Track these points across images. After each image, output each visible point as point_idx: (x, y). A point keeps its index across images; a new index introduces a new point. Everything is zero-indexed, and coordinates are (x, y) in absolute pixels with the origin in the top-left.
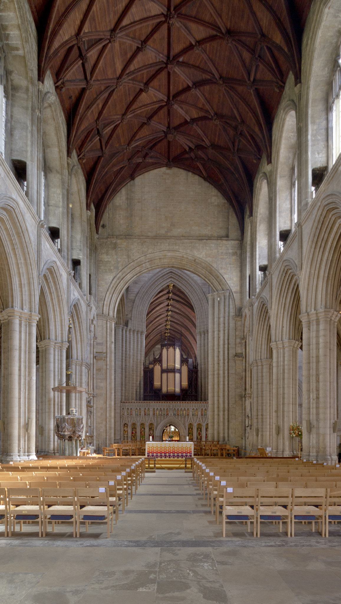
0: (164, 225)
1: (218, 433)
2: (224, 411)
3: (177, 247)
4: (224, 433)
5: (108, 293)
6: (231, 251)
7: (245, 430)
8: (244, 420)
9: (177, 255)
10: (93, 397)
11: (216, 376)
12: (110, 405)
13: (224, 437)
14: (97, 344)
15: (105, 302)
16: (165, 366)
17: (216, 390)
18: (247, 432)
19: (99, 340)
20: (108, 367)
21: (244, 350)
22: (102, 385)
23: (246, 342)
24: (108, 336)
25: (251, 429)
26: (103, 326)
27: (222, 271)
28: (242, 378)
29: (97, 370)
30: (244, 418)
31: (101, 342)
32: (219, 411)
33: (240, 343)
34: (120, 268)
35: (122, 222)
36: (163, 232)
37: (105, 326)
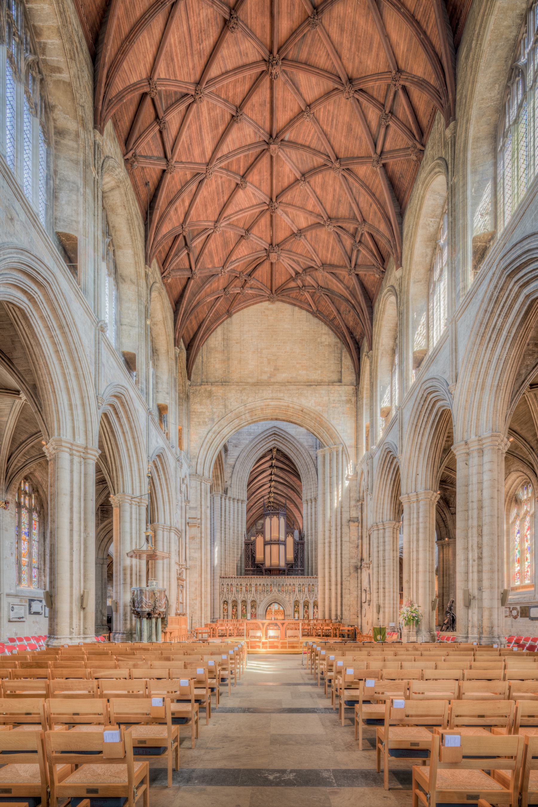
0: (266, 369)
1: (330, 610)
2: (336, 585)
3: (282, 395)
4: (336, 610)
5: (202, 449)
6: (344, 398)
7: (361, 607)
8: (359, 595)
9: (281, 404)
10: (186, 569)
11: (327, 545)
12: (206, 579)
13: (336, 615)
14: (190, 508)
15: (199, 460)
16: (268, 538)
17: (327, 561)
18: (363, 609)
19: (192, 504)
20: (203, 535)
21: (360, 514)
22: (197, 555)
23: (362, 504)
24: (203, 499)
25: (369, 605)
26: (196, 488)
27: (334, 422)
28: (358, 547)
29: (190, 538)
30: (359, 593)
31: (194, 506)
32: (330, 585)
33: (355, 506)
34: (216, 420)
35: (217, 366)
36: (265, 377)
37: (199, 488)
